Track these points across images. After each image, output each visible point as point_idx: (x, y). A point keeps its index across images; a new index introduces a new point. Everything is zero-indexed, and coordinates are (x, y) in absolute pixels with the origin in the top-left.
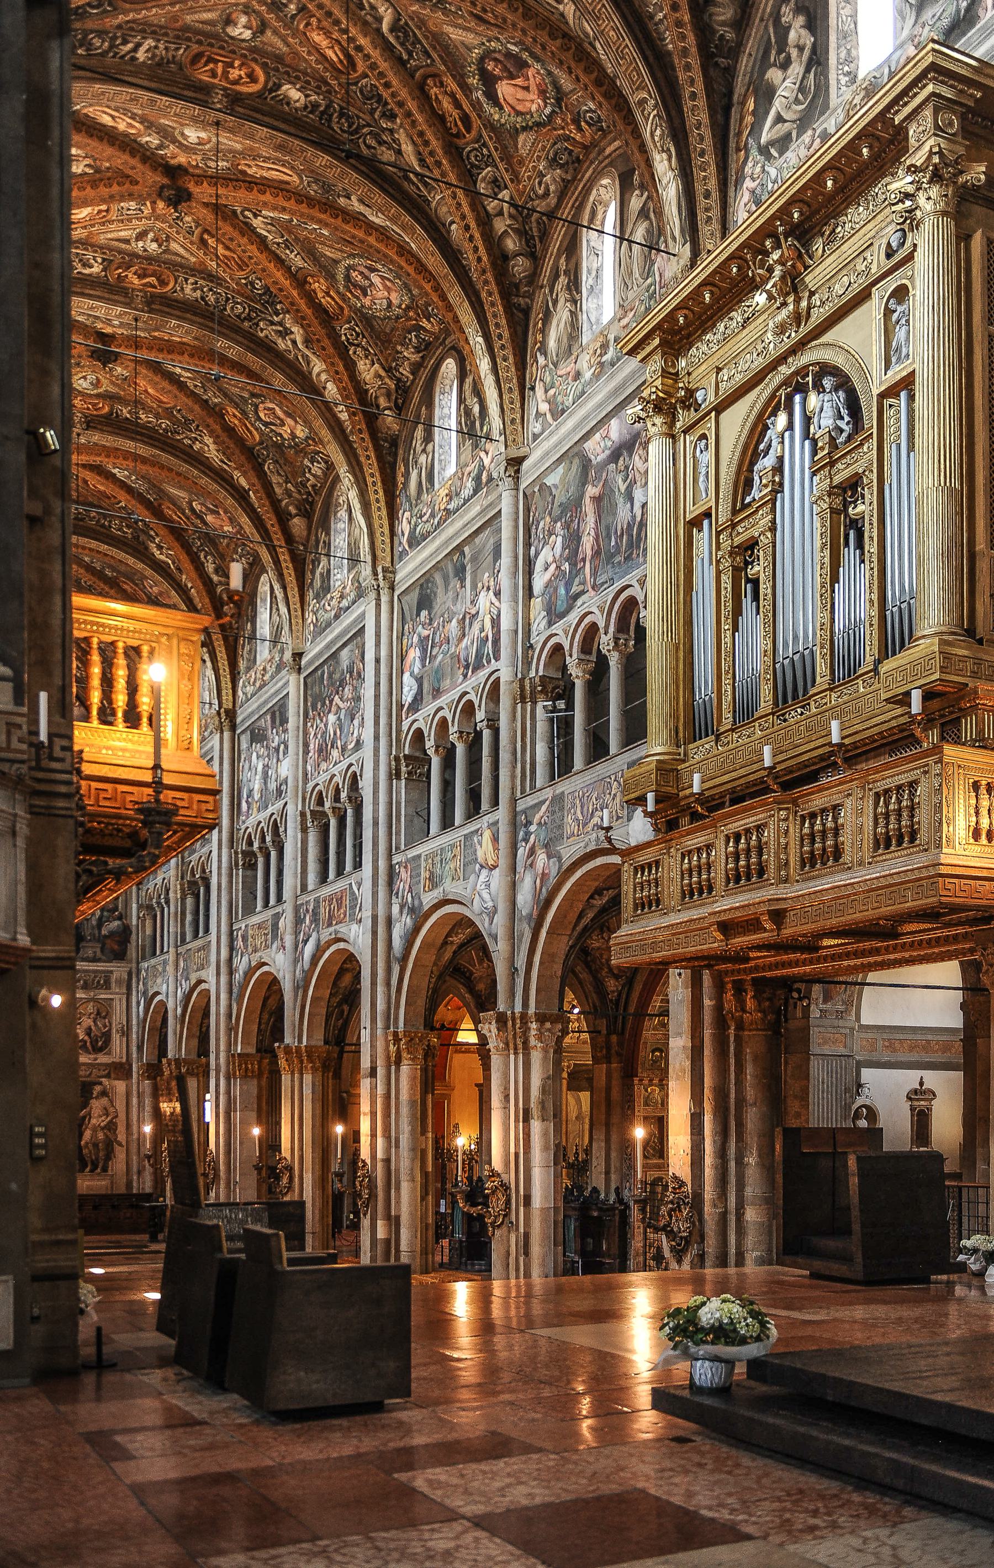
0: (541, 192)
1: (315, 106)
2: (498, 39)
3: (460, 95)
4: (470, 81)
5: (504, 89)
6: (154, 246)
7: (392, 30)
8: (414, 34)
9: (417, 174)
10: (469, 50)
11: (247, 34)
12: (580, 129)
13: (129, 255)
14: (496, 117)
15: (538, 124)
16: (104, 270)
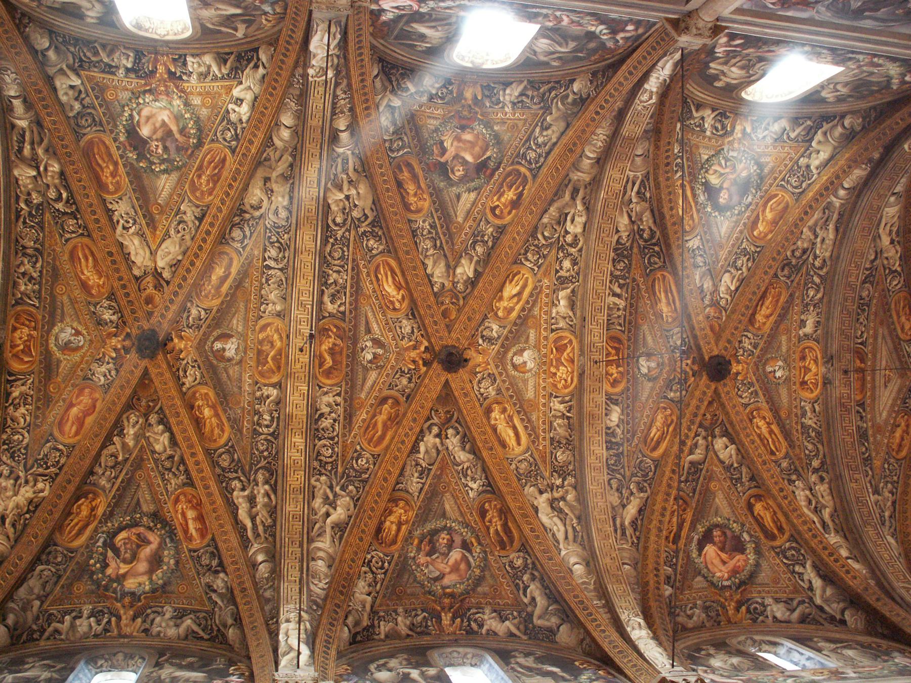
0: (689, 612)
1: (613, 434)
2: (743, 525)
3: (687, 525)
4: (699, 526)
5: (710, 550)
6: (369, 357)
7: (691, 463)
8: (699, 477)
9: (622, 525)
10: (716, 515)
11: (644, 370)
12: (737, 609)
13: (355, 335)
14: (694, 556)
15: (712, 583)
16: (331, 315)
